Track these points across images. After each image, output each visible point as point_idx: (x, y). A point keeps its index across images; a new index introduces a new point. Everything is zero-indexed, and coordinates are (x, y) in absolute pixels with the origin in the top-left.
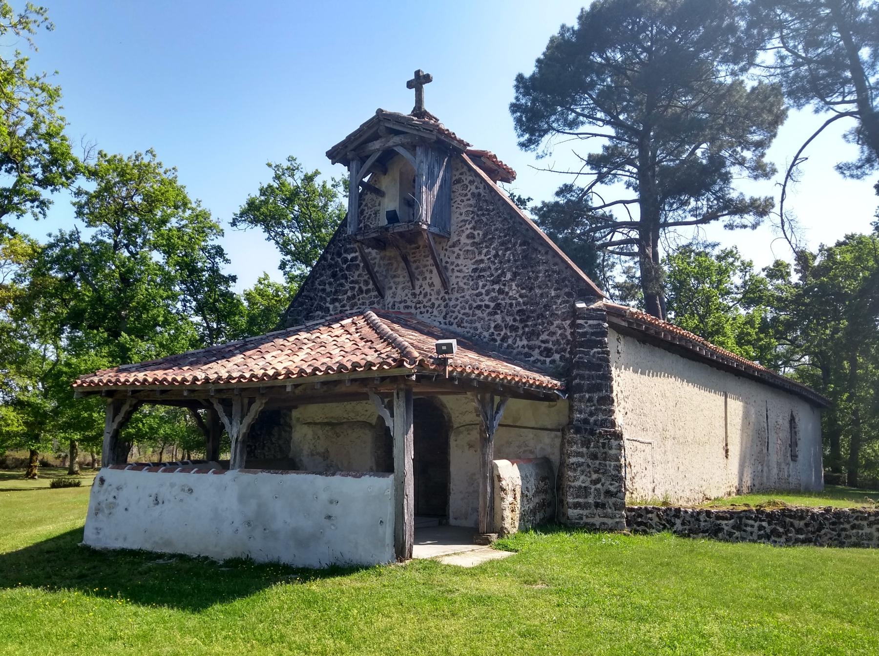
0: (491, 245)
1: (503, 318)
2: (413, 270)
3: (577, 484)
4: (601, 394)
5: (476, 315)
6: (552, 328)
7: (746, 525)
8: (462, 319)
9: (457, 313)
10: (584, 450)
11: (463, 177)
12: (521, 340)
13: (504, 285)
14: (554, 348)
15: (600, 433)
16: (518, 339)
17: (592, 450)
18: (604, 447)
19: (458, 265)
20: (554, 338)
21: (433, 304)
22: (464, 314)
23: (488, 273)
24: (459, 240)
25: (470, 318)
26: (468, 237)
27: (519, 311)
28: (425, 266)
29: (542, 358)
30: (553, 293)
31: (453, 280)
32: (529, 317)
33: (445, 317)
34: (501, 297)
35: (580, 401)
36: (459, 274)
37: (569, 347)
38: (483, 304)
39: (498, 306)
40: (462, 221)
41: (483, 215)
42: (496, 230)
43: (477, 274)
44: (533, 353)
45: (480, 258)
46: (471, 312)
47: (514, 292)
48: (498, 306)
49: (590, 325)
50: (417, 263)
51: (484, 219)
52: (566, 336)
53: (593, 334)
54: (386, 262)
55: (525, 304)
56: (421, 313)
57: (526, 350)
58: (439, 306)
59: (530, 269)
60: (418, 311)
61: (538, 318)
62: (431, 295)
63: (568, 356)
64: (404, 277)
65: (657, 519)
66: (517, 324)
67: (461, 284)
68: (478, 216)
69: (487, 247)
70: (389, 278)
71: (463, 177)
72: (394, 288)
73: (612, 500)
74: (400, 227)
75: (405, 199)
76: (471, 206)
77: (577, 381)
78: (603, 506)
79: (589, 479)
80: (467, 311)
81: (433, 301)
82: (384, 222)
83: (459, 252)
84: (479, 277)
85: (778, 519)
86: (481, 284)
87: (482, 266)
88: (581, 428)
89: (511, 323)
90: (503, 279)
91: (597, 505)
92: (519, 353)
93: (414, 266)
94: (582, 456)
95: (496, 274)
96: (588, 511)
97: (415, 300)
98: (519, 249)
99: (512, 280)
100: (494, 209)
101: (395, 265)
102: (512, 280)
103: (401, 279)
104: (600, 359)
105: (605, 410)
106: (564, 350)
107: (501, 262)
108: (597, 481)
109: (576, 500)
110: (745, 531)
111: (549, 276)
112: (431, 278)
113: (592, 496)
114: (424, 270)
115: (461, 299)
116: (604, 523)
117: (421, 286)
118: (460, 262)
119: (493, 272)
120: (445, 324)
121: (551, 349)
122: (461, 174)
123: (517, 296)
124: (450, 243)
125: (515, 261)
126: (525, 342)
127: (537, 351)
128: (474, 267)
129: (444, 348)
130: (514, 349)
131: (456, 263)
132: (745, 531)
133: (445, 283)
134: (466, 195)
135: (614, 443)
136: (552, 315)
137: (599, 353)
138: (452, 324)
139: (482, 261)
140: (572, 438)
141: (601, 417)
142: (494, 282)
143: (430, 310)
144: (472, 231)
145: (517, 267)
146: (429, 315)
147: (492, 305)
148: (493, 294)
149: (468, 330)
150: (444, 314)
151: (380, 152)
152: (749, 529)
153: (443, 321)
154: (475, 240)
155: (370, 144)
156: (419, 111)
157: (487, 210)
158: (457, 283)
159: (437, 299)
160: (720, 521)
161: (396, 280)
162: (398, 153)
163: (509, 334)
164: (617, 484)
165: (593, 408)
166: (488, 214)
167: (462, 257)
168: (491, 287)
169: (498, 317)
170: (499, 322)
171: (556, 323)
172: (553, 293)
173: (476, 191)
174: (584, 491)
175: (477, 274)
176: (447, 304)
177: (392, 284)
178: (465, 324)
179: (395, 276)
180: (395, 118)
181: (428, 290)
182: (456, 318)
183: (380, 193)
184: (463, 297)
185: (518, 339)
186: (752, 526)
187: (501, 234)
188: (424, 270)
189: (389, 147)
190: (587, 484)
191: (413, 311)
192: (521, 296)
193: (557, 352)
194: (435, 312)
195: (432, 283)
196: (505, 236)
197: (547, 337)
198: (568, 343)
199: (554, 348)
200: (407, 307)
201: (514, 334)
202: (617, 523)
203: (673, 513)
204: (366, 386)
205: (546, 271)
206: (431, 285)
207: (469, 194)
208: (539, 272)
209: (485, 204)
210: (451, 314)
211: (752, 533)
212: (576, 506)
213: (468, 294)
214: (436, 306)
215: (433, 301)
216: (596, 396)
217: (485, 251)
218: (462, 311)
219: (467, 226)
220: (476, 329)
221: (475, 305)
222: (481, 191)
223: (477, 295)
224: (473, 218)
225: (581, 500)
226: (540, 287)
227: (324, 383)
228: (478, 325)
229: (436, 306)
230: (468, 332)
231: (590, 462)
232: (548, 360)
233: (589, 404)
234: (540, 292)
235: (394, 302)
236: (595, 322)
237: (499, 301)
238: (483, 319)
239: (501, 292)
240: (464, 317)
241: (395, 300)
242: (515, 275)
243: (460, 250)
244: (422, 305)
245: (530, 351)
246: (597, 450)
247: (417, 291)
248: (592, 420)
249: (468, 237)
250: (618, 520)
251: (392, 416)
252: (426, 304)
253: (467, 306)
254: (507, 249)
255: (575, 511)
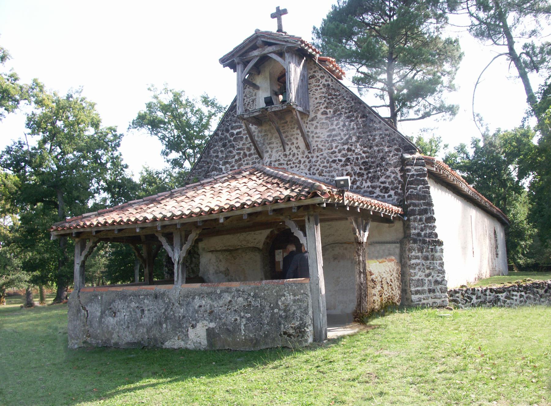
0: (339, 118)
1: (352, 168)
2: (284, 139)
3: (416, 277)
4: (427, 216)
5: (332, 167)
6: (388, 173)
7: (513, 295)
8: (322, 171)
9: (318, 167)
10: (420, 254)
11: (316, 74)
12: (366, 182)
13: (351, 145)
14: (390, 187)
15: (429, 241)
16: (364, 182)
17: (424, 254)
18: (432, 251)
19: (316, 133)
20: (390, 180)
21: (300, 161)
22: (323, 167)
23: (339, 138)
24: (316, 116)
25: (328, 169)
26: (322, 114)
27: (364, 162)
28: (292, 135)
29: (382, 194)
30: (386, 149)
31: (313, 144)
32: (370, 167)
33: (309, 170)
34: (350, 153)
35: (414, 221)
36: (317, 139)
37: (400, 185)
38: (337, 159)
39: (348, 160)
40: (317, 103)
41: (332, 98)
42: (343, 108)
43: (331, 139)
44: (375, 191)
45: (332, 128)
46: (328, 165)
47: (359, 150)
48: (348, 160)
49: (415, 170)
50: (286, 133)
51: (333, 101)
52: (398, 178)
53: (418, 175)
54: (263, 134)
55: (367, 157)
56: (291, 168)
57: (370, 189)
58: (304, 162)
59: (369, 134)
60: (289, 166)
61: (377, 167)
62: (298, 155)
63: (399, 191)
64: (277, 144)
65: (462, 297)
66: (362, 172)
67: (320, 146)
68: (328, 99)
69: (337, 120)
70: (266, 145)
71: (316, 74)
72: (270, 151)
73: (439, 287)
74: (276, 107)
75: (273, 91)
76: (323, 93)
77: (411, 208)
78: (434, 291)
79: (424, 274)
80: (325, 164)
81: (300, 159)
82: (262, 105)
83: (317, 124)
84: (333, 141)
85: (530, 290)
86: (334, 145)
87: (334, 133)
88: (416, 239)
89: (358, 171)
90: (350, 141)
91: (430, 291)
92: (365, 192)
93: (284, 135)
94: (419, 259)
95: (345, 138)
96: (424, 295)
97: (286, 159)
98: (360, 120)
99: (357, 142)
100: (340, 95)
101: (270, 136)
102: (357, 142)
103: (274, 145)
104: (424, 192)
105: (431, 226)
106: (397, 188)
107: (348, 130)
108: (428, 275)
109: (417, 289)
110: (512, 299)
111: (383, 138)
112: (297, 143)
113: (426, 285)
114: (292, 138)
115: (320, 157)
116: (435, 303)
117: (290, 149)
118: (318, 131)
119: (343, 137)
120: (310, 174)
121: (388, 187)
122: (315, 72)
123: (361, 152)
124: (310, 118)
125: (358, 128)
126: (369, 184)
127: (378, 189)
128: (329, 134)
129: (342, 183)
130: (362, 189)
131: (315, 132)
132: (512, 299)
133: (308, 146)
134: (319, 86)
135: (438, 248)
136: (387, 164)
137: (423, 188)
138: (315, 174)
139: (334, 130)
140: (412, 247)
141: (428, 231)
142: (344, 144)
143: (298, 165)
144: (325, 110)
145: (360, 133)
146: (297, 169)
147: (344, 159)
148: (344, 152)
149: (327, 177)
150: (308, 167)
151: (258, 58)
152: (514, 298)
153: (308, 172)
154: (328, 116)
155: (250, 53)
156: (280, 30)
157: (335, 95)
158: (317, 146)
159: (303, 157)
160: (498, 294)
161: (272, 146)
162: (270, 58)
163: (357, 179)
164: (442, 276)
165: (423, 225)
166: (336, 98)
167: (319, 127)
168: (342, 147)
169: (349, 168)
170: (350, 171)
171: (390, 170)
172: (386, 149)
173: (326, 83)
174: (421, 282)
175: (331, 139)
176: (310, 160)
177: (268, 149)
178: (325, 174)
179: (270, 143)
180: (268, 34)
181: (295, 151)
182: (318, 169)
183: (256, 87)
184: (322, 155)
185: (364, 182)
186: (516, 296)
187: (347, 111)
188: (292, 138)
189: (265, 54)
190: (423, 277)
191: (285, 166)
192: (364, 152)
193: (392, 189)
194: (302, 167)
195: (298, 146)
196: (350, 112)
197: (385, 180)
198: (399, 182)
199: (390, 187)
200: (281, 164)
201: (360, 179)
202: (443, 301)
203: (471, 292)
204: (282, 214)
205: (381, 134)
206: (298, 148)
207: (321, 85)
208: (375, 136)
209: (333, 91)
210: (314, 167)
211: (516, 300)
212: (417, 292)
213: (325, 153)
214: (302, 162)
215: (300, 159)
216: (424, 217)
217: (335, 123)
218: (322, 165)
219: (321, 106)
220: (333, 177)
221: (331, 160)
222: (330, 83)
223: (332, 153)
224: (325, 101)
225: (419, 288)
226: (377, 146)
227: (250, 215)
228: (334, 174)
229: (302, 162)
230: (327, 179)
231: (424, 262)
232: (386, 195)
233: (420, 223)
234: (377, 149)
235: (271, 161)
236: (419, 167)
237: (348, 157)
238: (338, 169)
239: (349, 150)
240: (323, 168)
241: (272, 159)
242: (359, 138)
243: (317, 123)
244: (292, 162)
245: (373, 190)
246: (428, 254)
247: (287, 152)
248: (423, 233)
249: (322, 114)
250: (443, 299)
251: (305, 235)
252: (295, 162)
253: (325, 161)
254: (352, 121)
255: (416, 296)
